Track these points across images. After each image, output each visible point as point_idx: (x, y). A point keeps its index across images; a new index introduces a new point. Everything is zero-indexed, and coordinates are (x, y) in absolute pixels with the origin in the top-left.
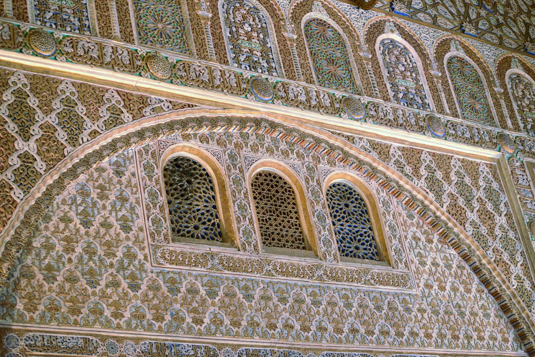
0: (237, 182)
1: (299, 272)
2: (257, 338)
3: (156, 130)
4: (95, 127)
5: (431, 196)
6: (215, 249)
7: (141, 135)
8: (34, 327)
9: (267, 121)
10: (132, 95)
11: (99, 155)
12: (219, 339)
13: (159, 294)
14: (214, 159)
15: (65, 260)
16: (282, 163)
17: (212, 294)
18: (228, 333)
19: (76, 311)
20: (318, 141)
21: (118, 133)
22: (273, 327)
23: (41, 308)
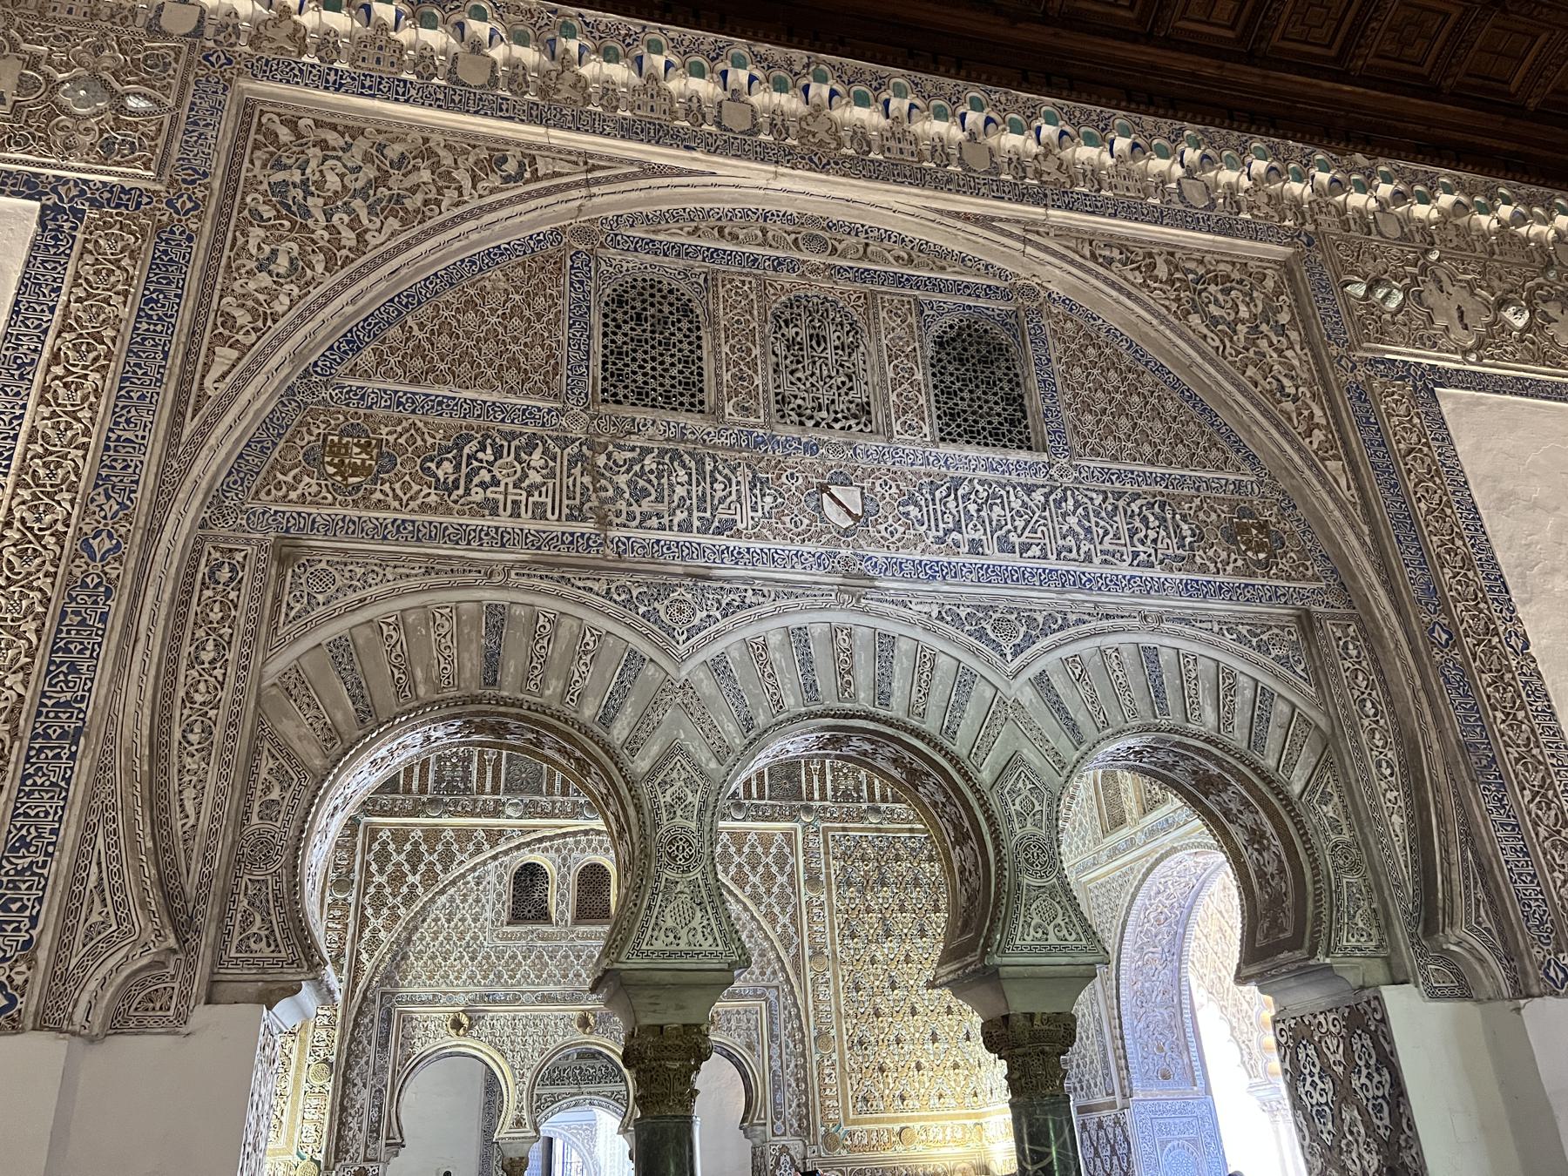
0: (564, 877)
3: (506, 853)
7: (495, 858)
11: (463, 876)
12: (525, 987)
21: (478, 859)
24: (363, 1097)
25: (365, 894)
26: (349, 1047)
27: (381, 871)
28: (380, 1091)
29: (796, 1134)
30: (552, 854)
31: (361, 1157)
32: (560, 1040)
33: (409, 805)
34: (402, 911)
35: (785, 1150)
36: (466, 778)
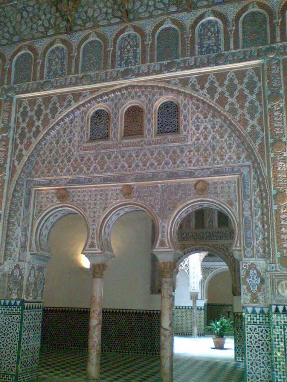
0: (115, 114)
1: (133, 145)
2: (109, 173)
3: (83, 105)
4: (61, 110)
5: (208, 96)
6: (100, 143)
7: (78, 108)
8: (37, 179)
9: (131, 86)
10: (77, 93)
11: (62, 120)
13: (77, 162)
14: (108, 107)
15: (49, 157)
16: (137, 101)
17: (95, 159)
18: (99, 173)
19: (49, 172)
20: (153, 87)
22: (116, 167)
23: (39, 173)
24: (18, 231)
25: (17, 133)
26: (10, 207)
27: (24, 121)
28: (26, 228)
29: (262, 257)
30: (109, 103)
31: (17, 259)
32: (114, 202)
33: (35, 86)
34: (33, 140)
35: (253, 266)
36: (62, 69)
